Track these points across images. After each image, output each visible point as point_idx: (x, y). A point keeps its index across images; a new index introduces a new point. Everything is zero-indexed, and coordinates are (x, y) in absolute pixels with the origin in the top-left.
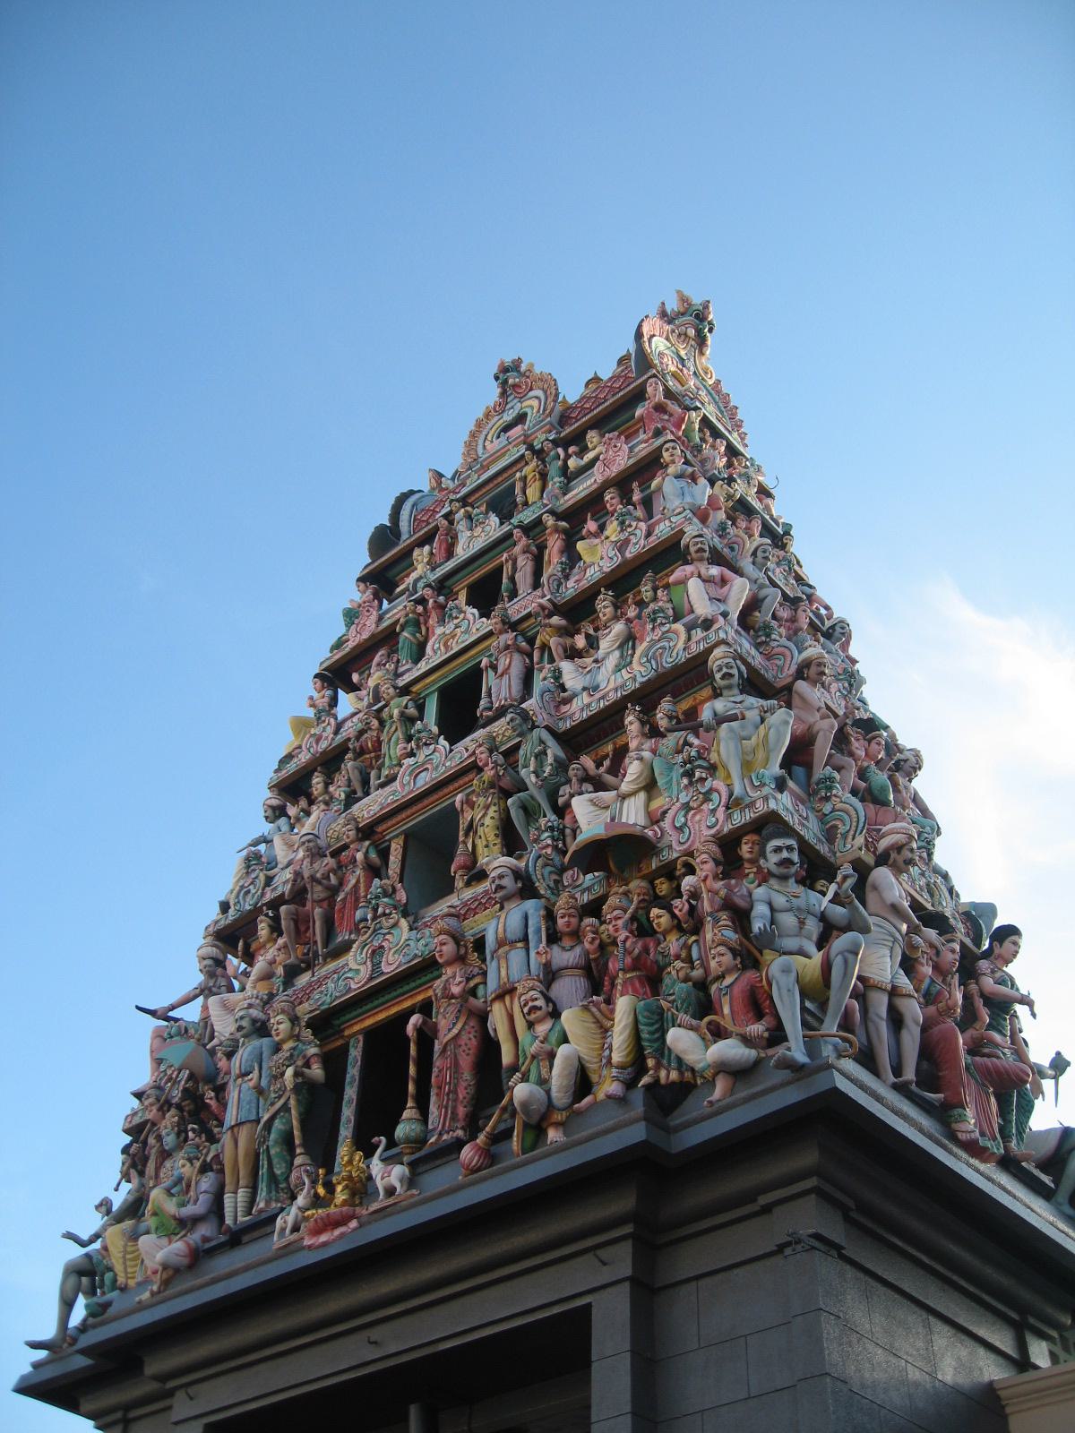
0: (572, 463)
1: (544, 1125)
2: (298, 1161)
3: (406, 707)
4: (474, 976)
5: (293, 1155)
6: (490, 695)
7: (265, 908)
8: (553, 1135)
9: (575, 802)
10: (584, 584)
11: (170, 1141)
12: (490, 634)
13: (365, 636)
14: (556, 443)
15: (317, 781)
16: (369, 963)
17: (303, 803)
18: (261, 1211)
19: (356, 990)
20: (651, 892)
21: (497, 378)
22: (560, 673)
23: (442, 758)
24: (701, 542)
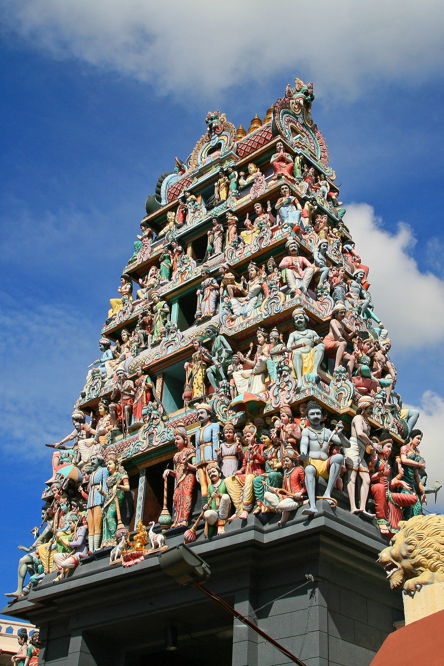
0: (243, 182)
1: (217, 526)
3: (163, 307)
4: (191, 453)
6: (200, 309)
7: (102, 399)
8: (221, 531)
9: (235, 374)
10: (243, 257)
11: (64, 507)
14: (234, 168)
16: (147, 440)
18: (104, 547)
19: (142, 451)
20: (264, 422)
24: (294, 246)
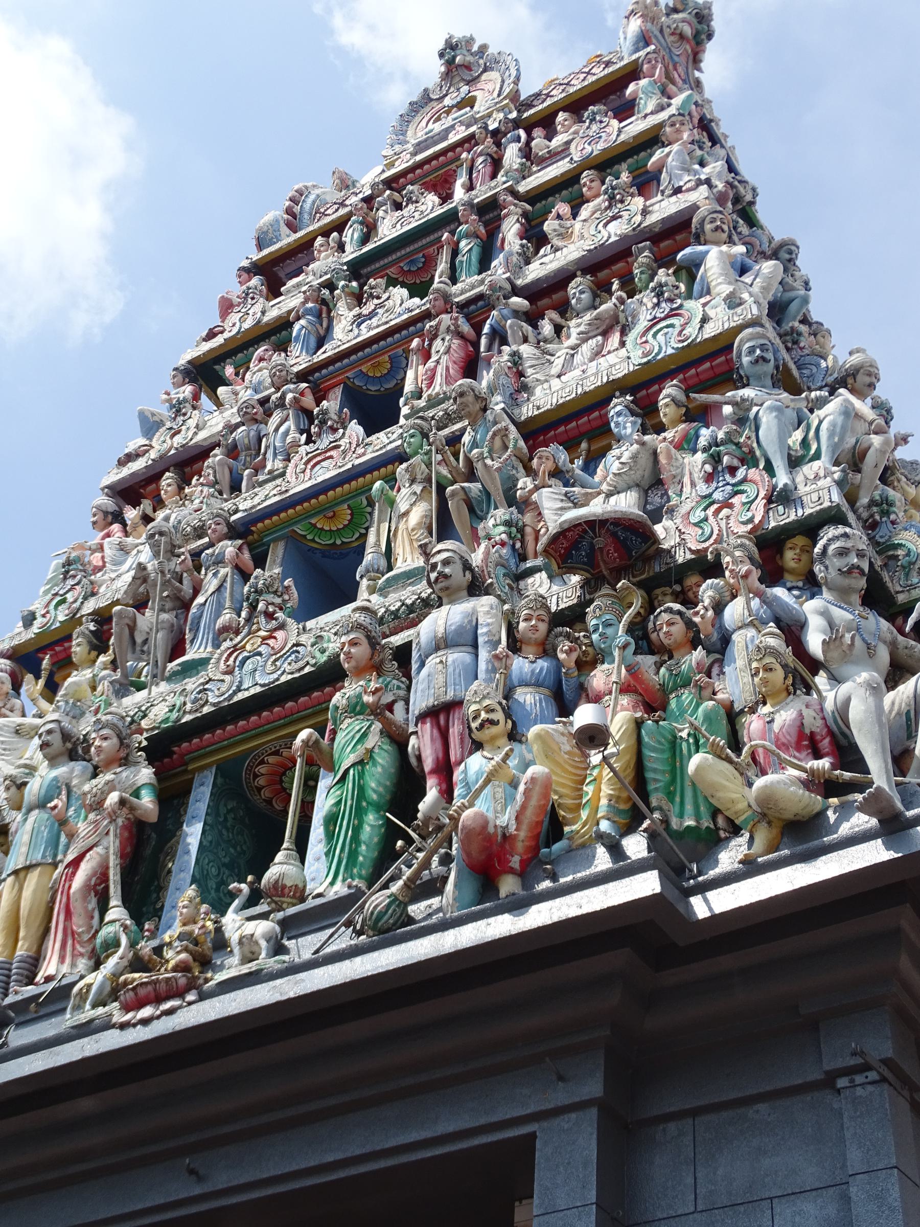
2: (110, 915)
5: (103, 907)
12: (427, 315)
13: (247, 325)
15: (168, 481)
17: (146, 505)
18: (48, 979)
21: (441, 55)
22: (520, 358)
23: (355, 445)
